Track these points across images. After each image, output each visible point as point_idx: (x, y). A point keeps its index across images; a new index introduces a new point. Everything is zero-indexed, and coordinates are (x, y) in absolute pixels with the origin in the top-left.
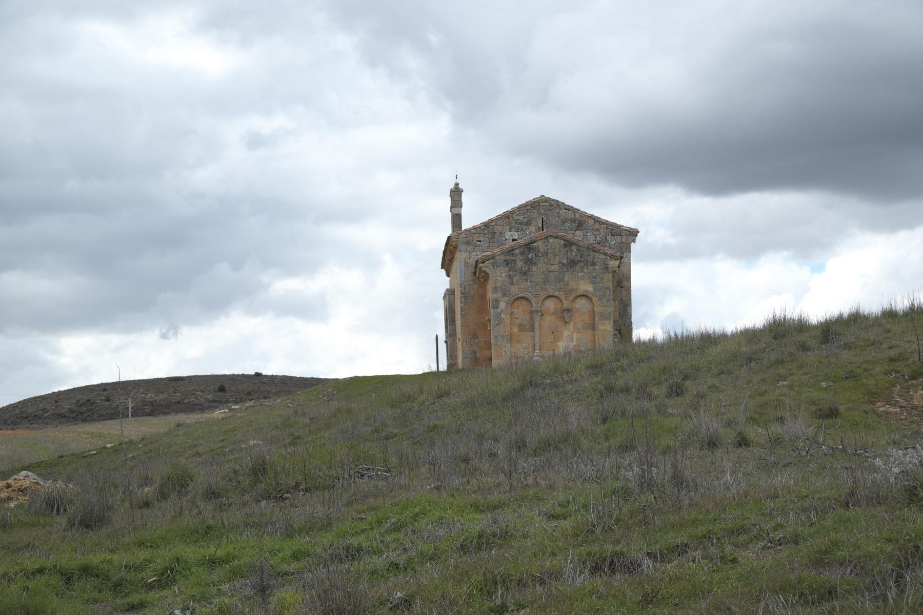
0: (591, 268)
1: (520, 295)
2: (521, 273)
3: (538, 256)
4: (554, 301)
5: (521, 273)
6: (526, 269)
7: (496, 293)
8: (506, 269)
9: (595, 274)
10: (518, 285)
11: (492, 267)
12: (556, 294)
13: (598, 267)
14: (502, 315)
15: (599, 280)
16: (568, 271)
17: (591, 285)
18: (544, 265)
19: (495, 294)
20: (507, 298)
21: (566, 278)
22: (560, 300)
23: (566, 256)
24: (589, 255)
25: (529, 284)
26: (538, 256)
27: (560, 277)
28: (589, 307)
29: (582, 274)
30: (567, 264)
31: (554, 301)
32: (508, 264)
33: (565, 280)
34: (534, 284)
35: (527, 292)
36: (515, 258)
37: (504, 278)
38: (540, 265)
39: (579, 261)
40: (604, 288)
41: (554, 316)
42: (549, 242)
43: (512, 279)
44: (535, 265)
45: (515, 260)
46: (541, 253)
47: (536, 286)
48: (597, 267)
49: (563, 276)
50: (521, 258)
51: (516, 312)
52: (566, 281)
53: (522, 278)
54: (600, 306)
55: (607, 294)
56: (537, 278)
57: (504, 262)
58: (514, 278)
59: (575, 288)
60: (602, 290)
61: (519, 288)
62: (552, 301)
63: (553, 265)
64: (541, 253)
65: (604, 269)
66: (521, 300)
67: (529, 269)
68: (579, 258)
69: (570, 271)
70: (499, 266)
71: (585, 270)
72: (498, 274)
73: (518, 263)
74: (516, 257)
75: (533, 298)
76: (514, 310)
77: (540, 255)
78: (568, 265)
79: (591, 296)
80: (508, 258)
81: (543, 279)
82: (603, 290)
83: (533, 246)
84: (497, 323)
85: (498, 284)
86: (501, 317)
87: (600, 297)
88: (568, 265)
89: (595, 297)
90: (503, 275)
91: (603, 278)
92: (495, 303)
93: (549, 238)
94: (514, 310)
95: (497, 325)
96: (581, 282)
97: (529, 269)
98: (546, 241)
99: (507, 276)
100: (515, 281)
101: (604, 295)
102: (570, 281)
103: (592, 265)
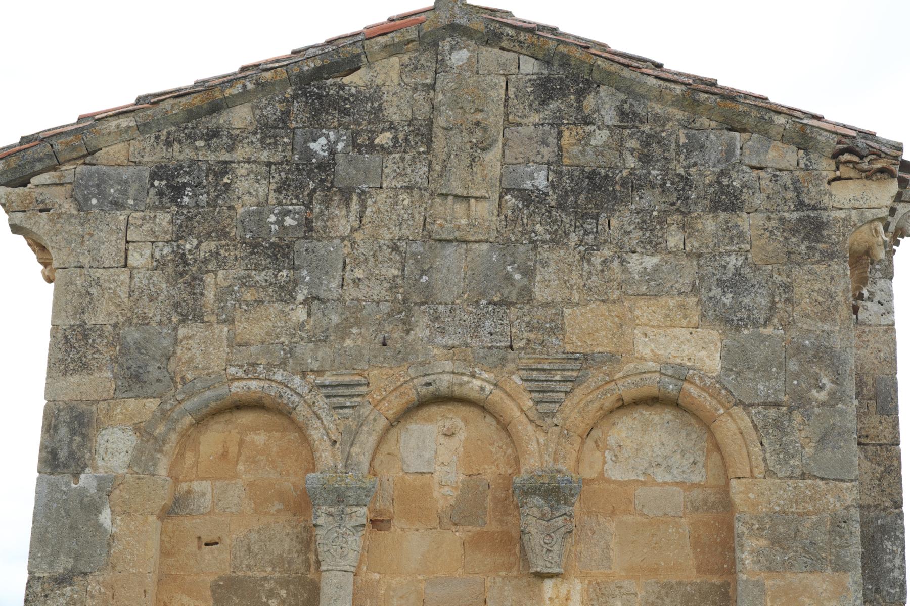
0: (709, 224)
1: (237, 388)
2: (254, 245)
3: (371, 148)
4: (462, 436)
5: (254, 245)
6: (289, 221)
7: (83, 366)
8: (163, 219)
9: (733, 261)
10: (230, 321)
11: (69, 207)
12: (474, 386)
13: (758, 219)
14: (105, 517)
15: (764, 301)
16: (557, 241)
17: (713, 335)
18: (405, 199)
19: (74, 379)
20: (152, 404)
21: (547, 283)
22: (505, 426)
23: (548, 153)
24: (694, 146)
25: (301, 314)
26: (371, 148)
27: (508, 278)
28: (696, 478)
29: (650, 262)
30: (552, 199)
31: (462, 436)
32: (179, 190)
33: (540, 293)
34: (335, 319)
35: (283, 364)
36: (226, 157)
37: (140, 280)
38: (379, 201)
39: (635, 184)
40: (799, 349)
41: (460, 534)
42: (441, 65)
43: (195, 284)
44: (347, 202)
45: (225, 168)
46: (392, 127)
47: (343, 331)
48: (747, 222)
49: (529, 273)
50: (264, 155)
51: (207, 502)
52: (545, 305)
53: (259, 277)
54: (769, 473)
55: (822, 396)
56: (357, 282)
57: (154, 176)
58: (209, 279)
59: (603, 345)
60: (782, 365)
61: (235, 343)
62: (449, 435)
63: (466, 198)
64: (392, 127)
65: (794, 231)
66: (246, 418)
67: (308, 225)
68: (632, 162)
69: (574, 238)
70: (118, 205)
71: (674, 240)
72: (109, 251)
73: (241, 186)
74: (231, 149)
75: (322, 402)
76: (197, 486)
77: (384, 139)
78: (561, 206)
79: (706, 401)
80: (181, 154)
81: (393, 288)
82: (793, 366)
83: (342, 87)
84: (63, 564)
85: (99, 317)
86: (99, 526)
87: (772, 412)
88: (561, 206)
89: (738, 411)
90: (135, 259)
91: (787, 288)
92: (63, 431)
93: (445, 45)
94: (197, 486)
95: (62, 581)
96: (644, 310)
97: (308, 225)
98: (425, 59)
99: (159, 265)
100: (210, 295)
101: (801, 402)
102: (569, 302)
103: (715, 207)
